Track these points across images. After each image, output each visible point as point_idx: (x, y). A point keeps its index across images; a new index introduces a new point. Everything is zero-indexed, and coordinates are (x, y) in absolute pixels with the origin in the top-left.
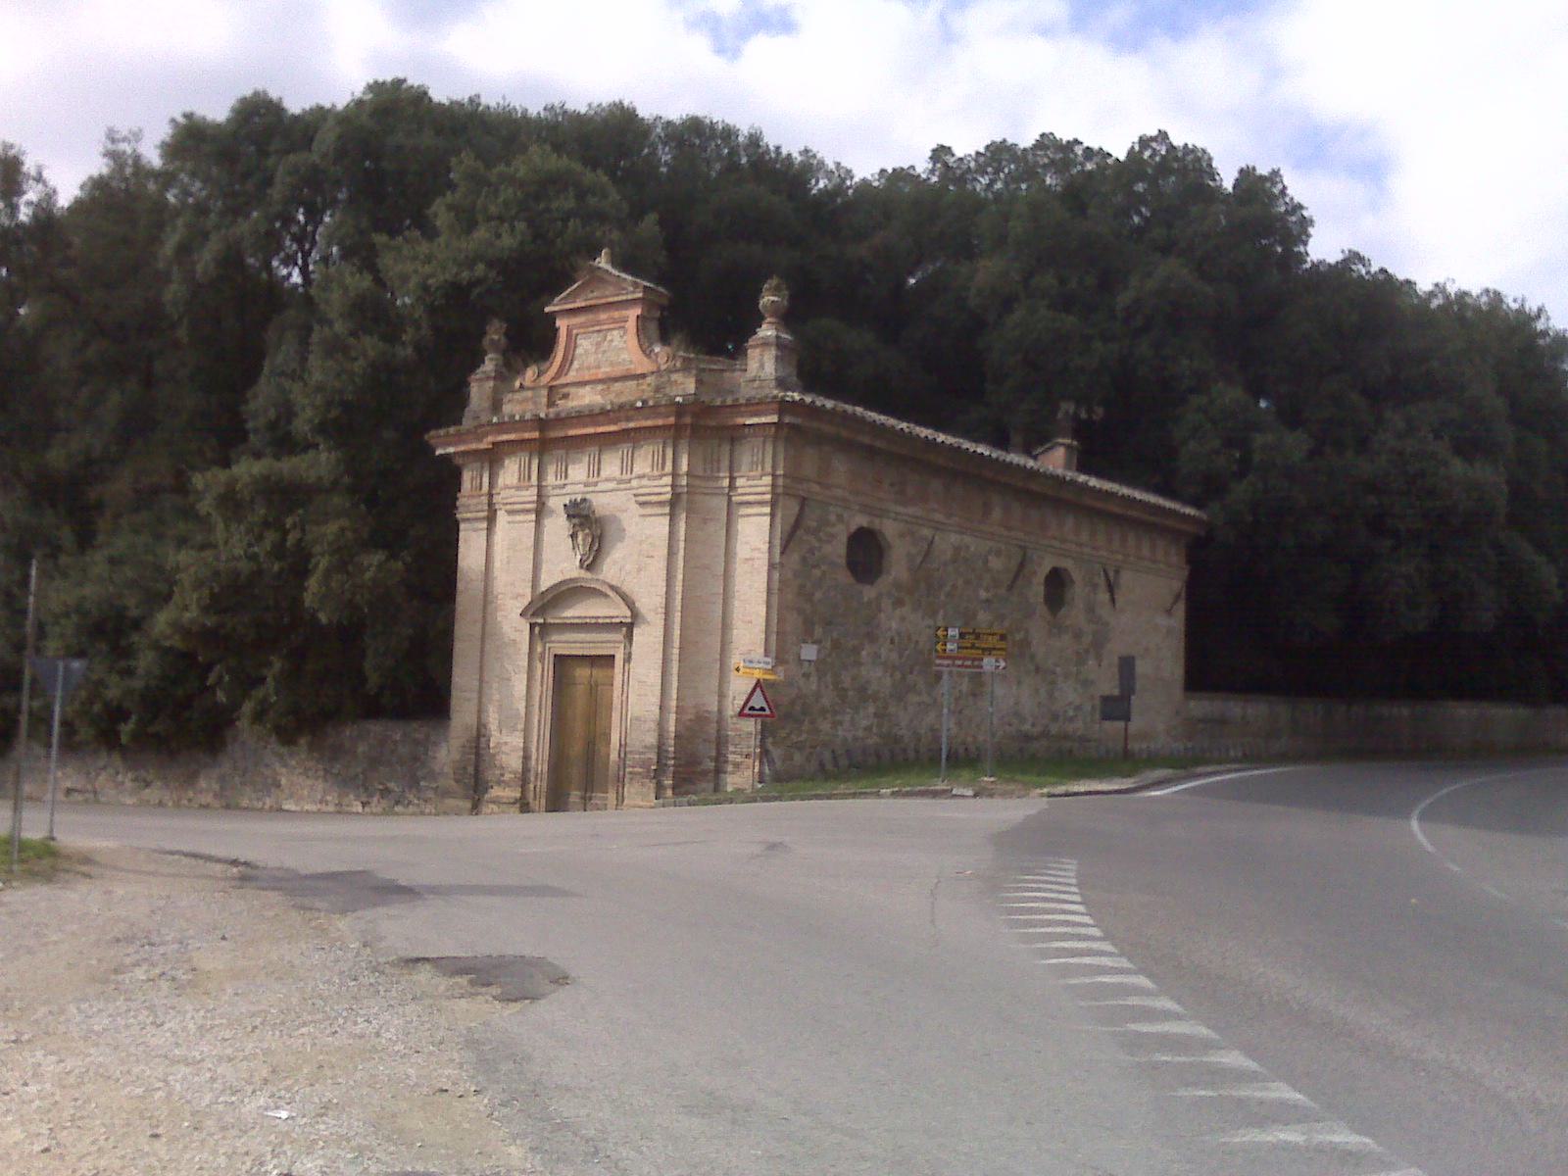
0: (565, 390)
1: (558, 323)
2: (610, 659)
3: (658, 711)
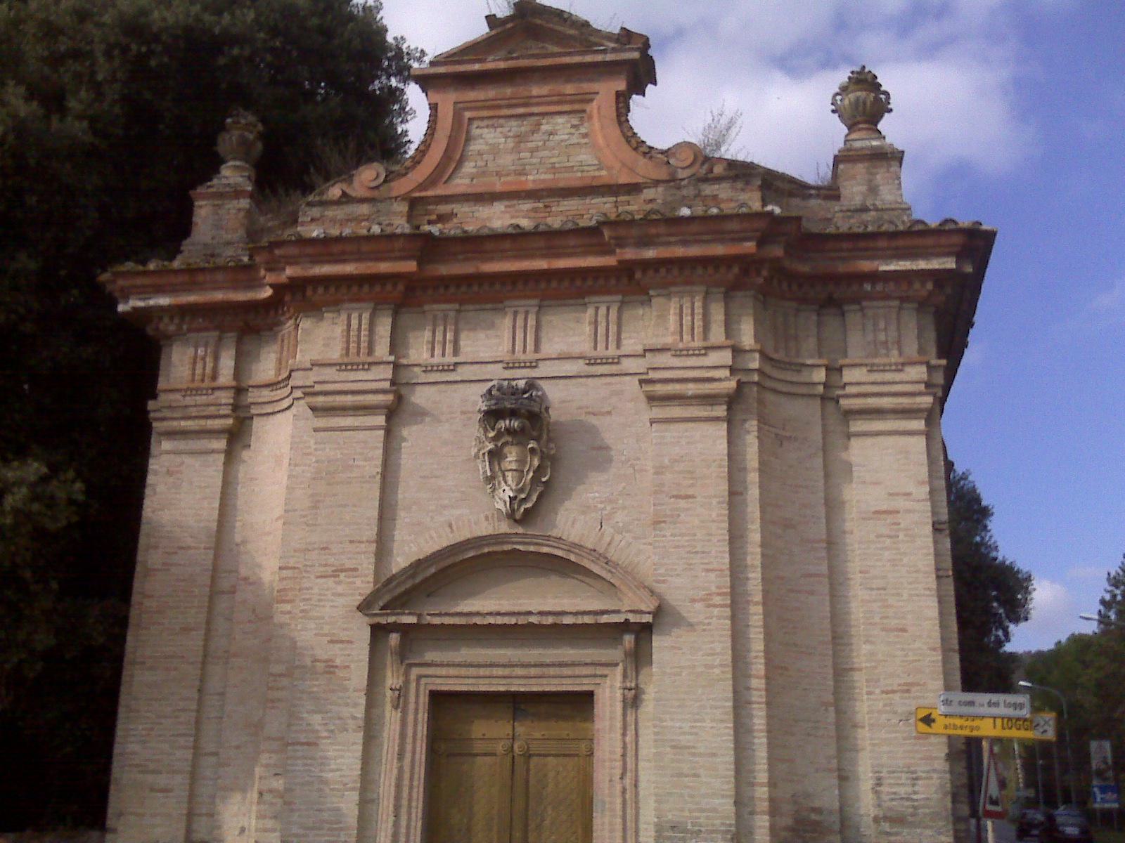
0: (444, 209)
2: (581, 703)
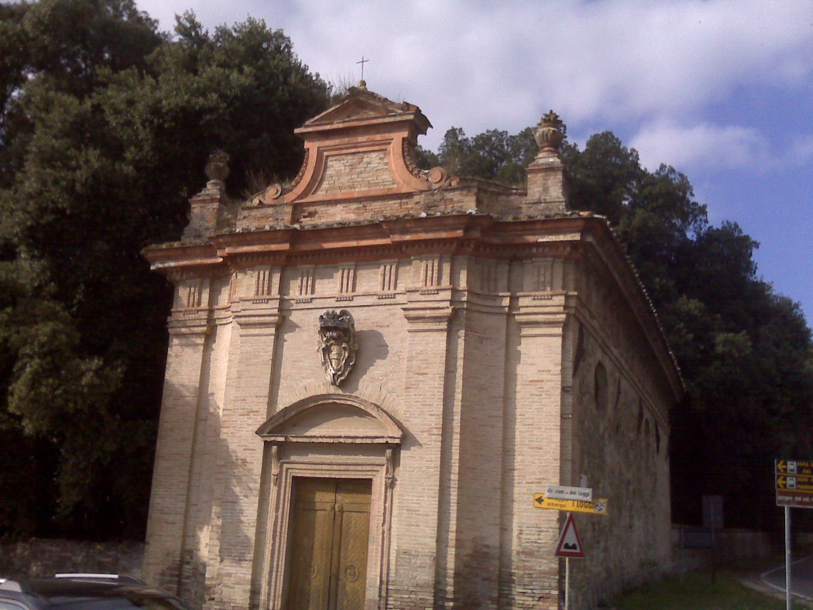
0: (311, 209)
1: (307, 145)
2: (364, 485)
3: (434, 544)
